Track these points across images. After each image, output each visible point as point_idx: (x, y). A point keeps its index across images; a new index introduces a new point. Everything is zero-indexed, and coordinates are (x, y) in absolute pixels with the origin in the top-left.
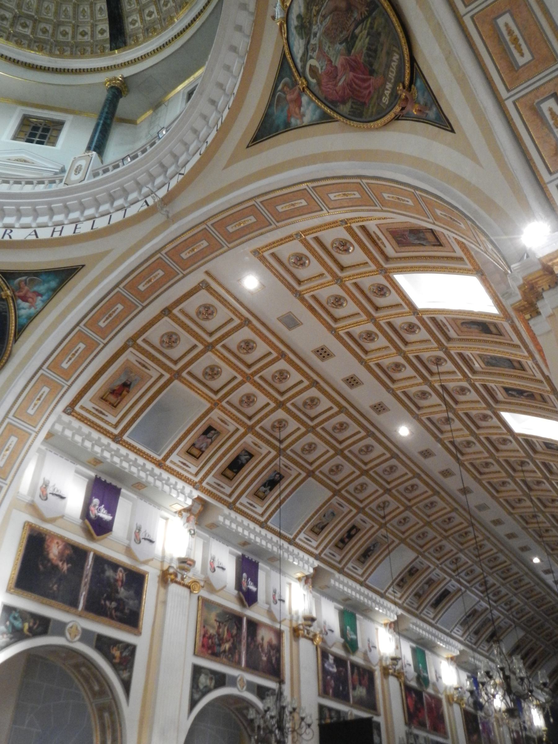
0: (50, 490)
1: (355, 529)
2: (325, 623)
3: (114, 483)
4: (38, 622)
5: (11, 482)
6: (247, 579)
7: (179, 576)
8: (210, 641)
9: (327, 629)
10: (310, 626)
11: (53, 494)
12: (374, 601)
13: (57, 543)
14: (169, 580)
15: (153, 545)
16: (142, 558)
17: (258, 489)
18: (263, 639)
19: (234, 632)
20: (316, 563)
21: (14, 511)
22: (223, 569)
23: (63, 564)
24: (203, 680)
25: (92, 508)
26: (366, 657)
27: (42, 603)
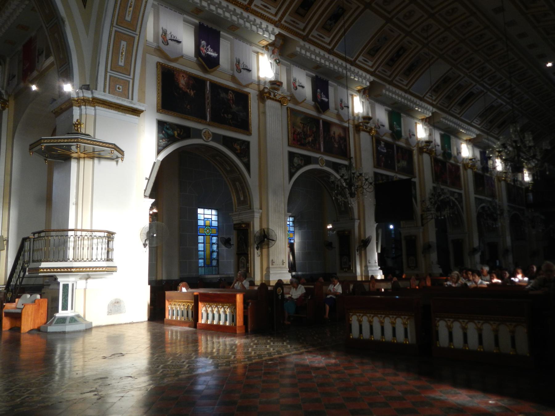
0: (169, 37)
2: (378, 120)
3: (214, 27)
4: (182, 130)
5: (140, 33)
6: (321, 93)
7: (272, 94)
8: (298, 136)
9: (379, 125)
10: (368, 123)
11: (171, 40)
12: (415, 103)
13: (183, 76)
14: (266, 97)
15: (251, 72)
16: (244, 83)
18: (334, 133)
19: (314, 129)
20: (372, 79)
21: (148, 55)
22: (303, 87)
23: (190, 91)
24: (296, 160)
25: (202, 48)
26: (407, 141)
27: (182, 118)
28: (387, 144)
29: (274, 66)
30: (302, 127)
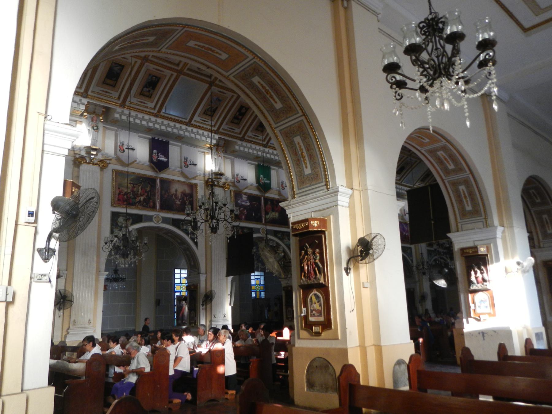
1: (244, 109)
8: (125, 196)
17: (142, 90)
18: (176, 191)
24: (121, 219)
28: (251, 198)
29: (91, 132)
30: (131, 188)
